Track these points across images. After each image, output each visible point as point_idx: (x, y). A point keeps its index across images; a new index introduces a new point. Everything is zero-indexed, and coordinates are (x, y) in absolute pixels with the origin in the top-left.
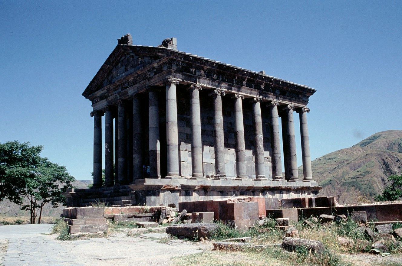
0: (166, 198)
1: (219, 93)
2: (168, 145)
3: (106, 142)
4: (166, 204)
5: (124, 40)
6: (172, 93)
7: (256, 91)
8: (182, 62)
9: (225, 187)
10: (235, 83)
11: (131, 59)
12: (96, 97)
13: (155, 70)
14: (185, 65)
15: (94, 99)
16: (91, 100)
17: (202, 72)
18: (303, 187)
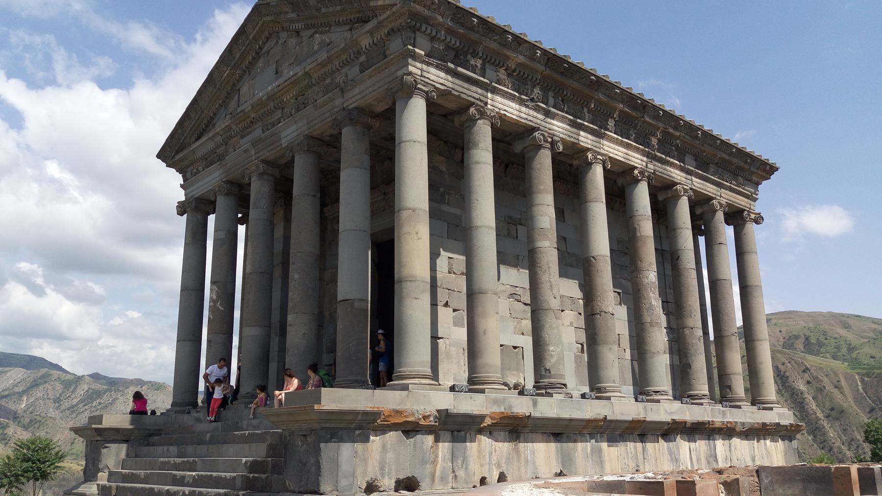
0: (390, 456)
1: (546, 141)
2: (400, 282)
3: (213, 282)
4: (390, 478)
6: (415, 122)
7: (637, 150)
8: (450, 31)
9: (571, 420)
10: (587, 117)
11: (293, 41)
13: (363, 58)
14: (455, 42)
15: (187, 167)
16: (180, 171)
17: (502, 74)
18: (764, 424)
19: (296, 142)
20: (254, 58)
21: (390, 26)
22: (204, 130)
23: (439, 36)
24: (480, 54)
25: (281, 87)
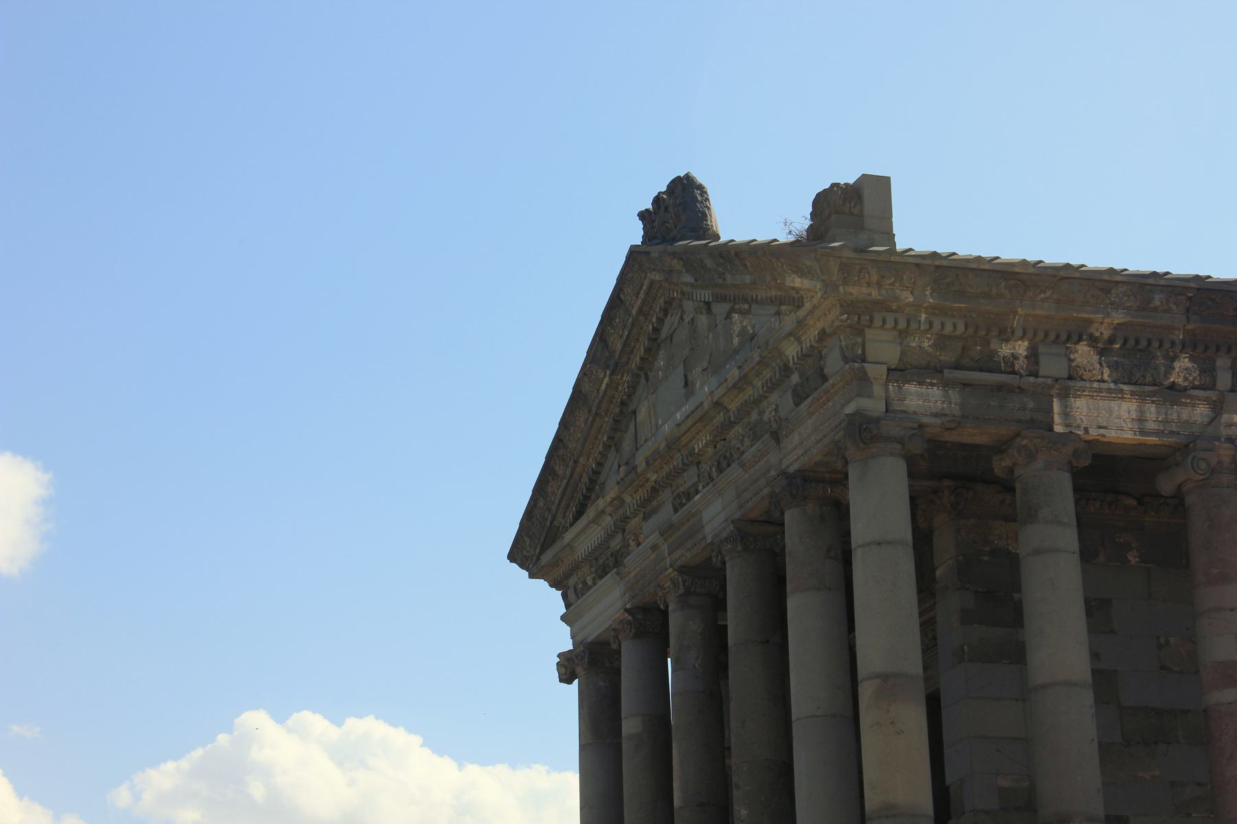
5: (678, 210)
11: (703, 320)
12: (575, 568)
13: (795, 378)
15: (567, 576)
16: (555, 584)
17: (1083, 354)
19: (724, 534)
20: (648, 350)
21: (820, 325)
22: (586, 498)
23: (913, 326)
24: (1019, 333)
25: (684, 428)
